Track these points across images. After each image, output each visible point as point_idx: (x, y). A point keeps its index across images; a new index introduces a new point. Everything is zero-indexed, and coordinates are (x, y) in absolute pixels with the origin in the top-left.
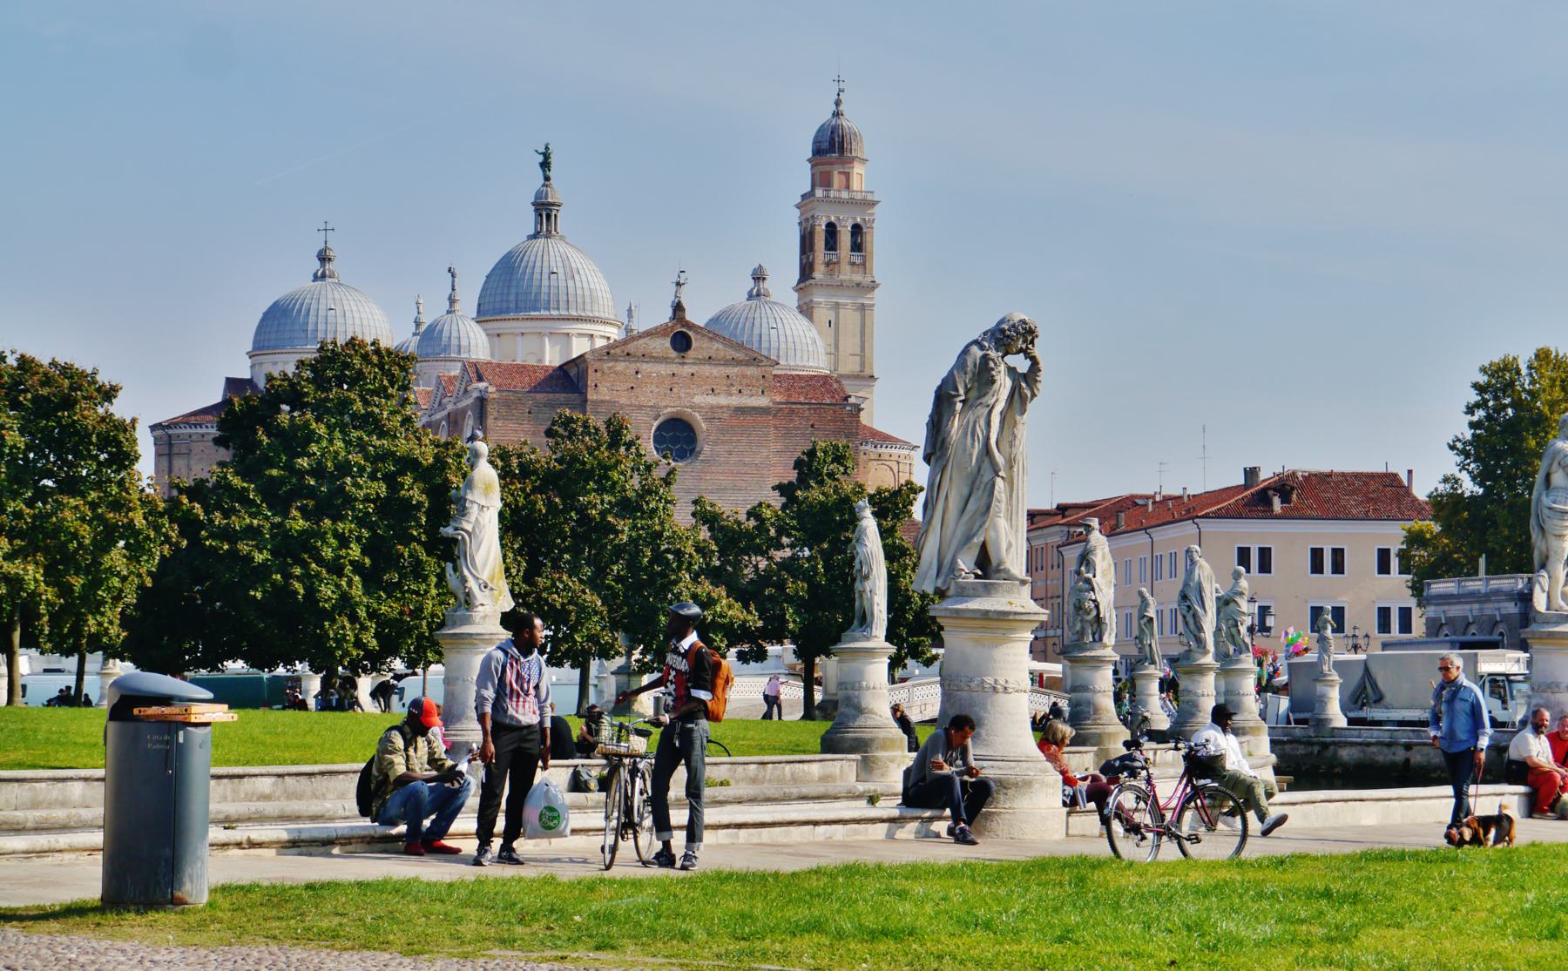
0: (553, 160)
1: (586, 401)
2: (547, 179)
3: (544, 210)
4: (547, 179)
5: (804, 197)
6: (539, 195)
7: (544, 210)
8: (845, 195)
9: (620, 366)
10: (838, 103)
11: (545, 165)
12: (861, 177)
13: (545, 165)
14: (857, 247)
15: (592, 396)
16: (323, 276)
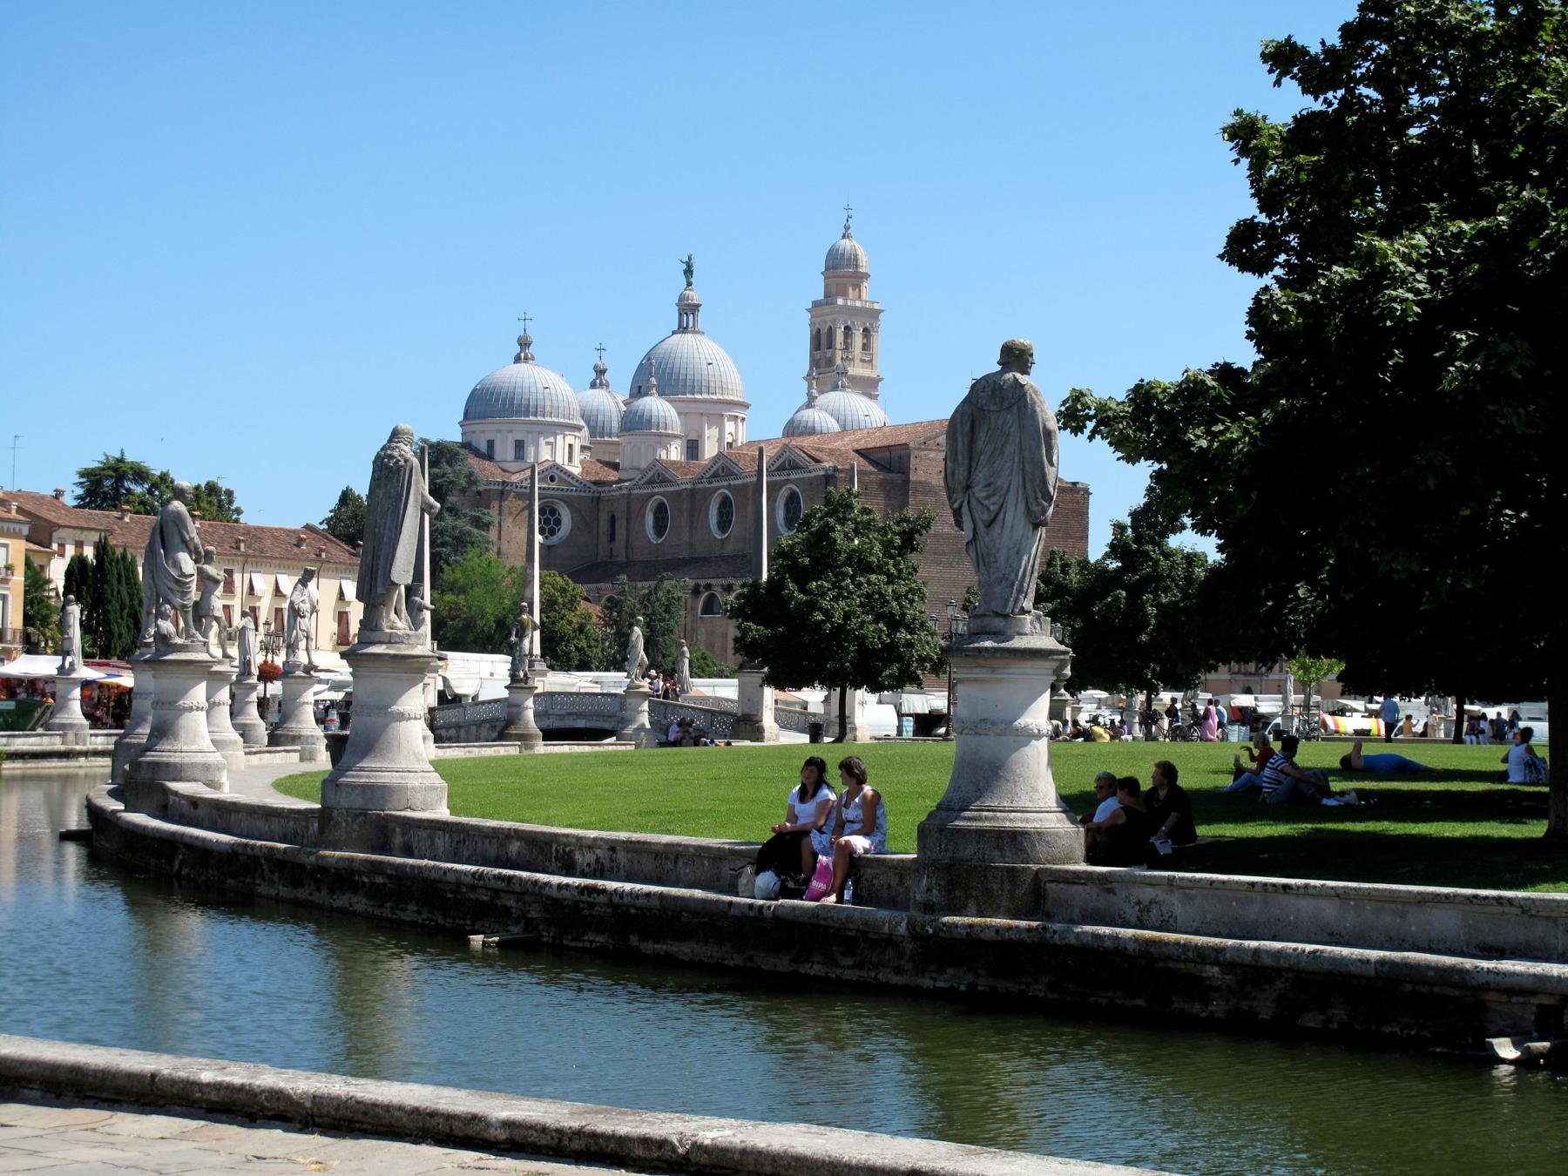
0: (695, 269)
1: (907, 481)
2: (689, 284)
3: (688, 309)
4: (689, 284)
5: (816, 304)
6: (682, 298)
7: (688, 309)
8: (858, 304)
9: (932, 455)
10: (847, 228)
11: (689, 272)
12: (869, 293)
13: (689, 272)
14: (866, 347)
15: (913, 478)
16: (526, 359)
